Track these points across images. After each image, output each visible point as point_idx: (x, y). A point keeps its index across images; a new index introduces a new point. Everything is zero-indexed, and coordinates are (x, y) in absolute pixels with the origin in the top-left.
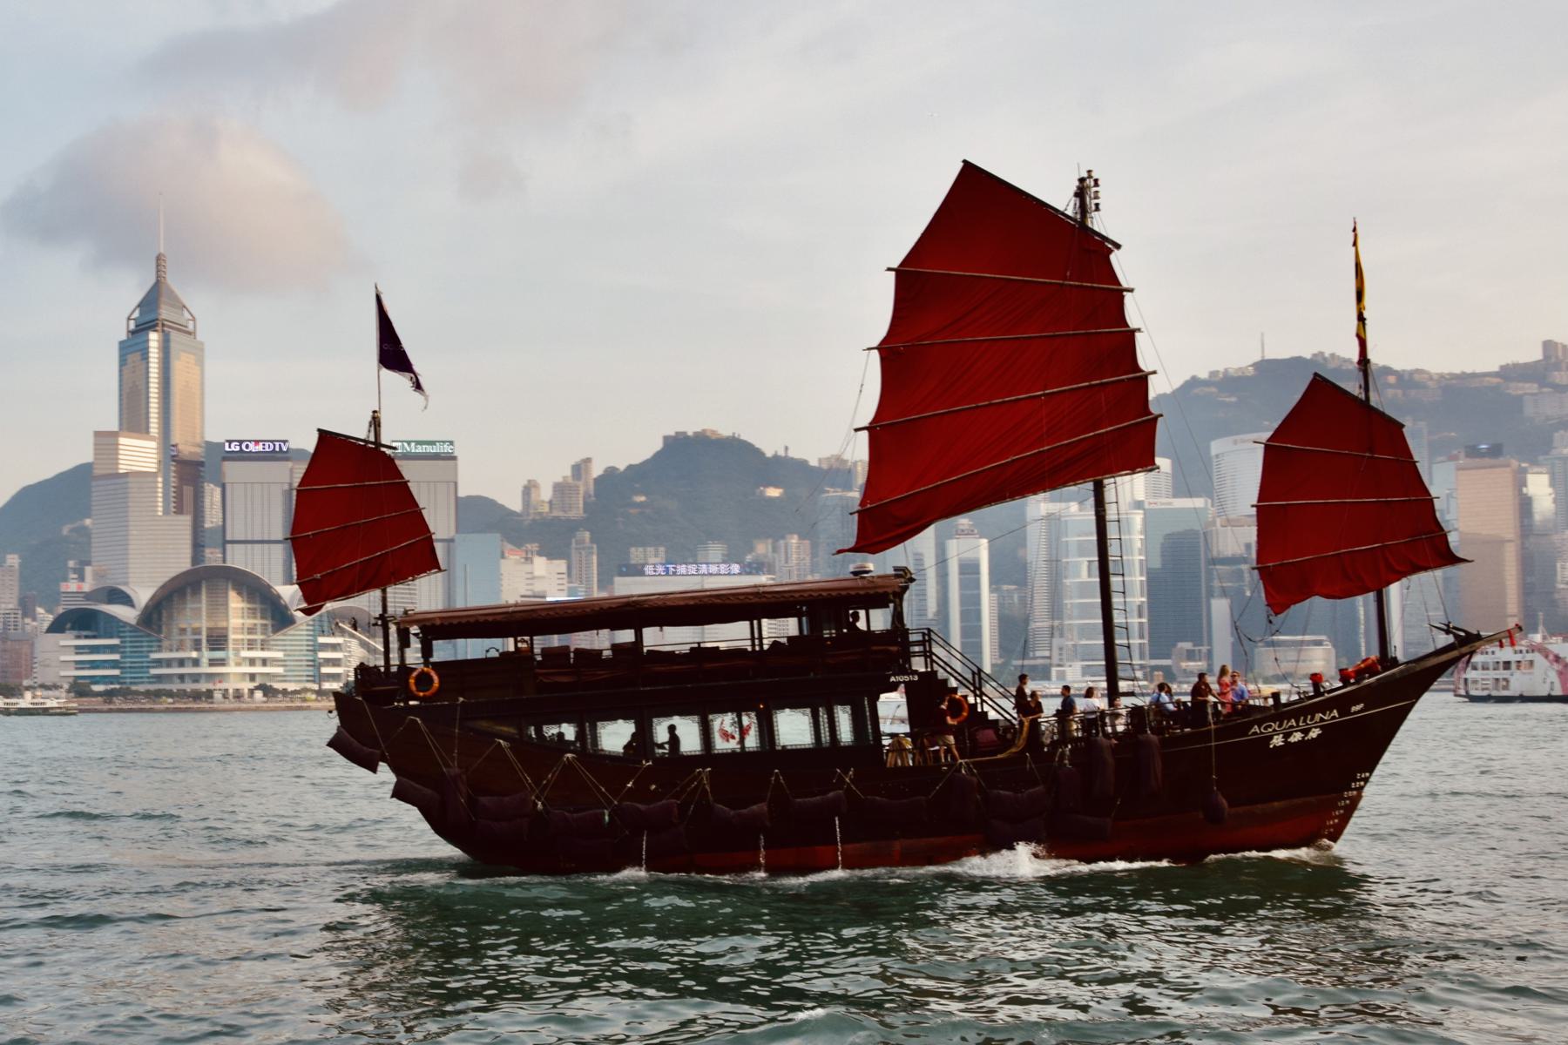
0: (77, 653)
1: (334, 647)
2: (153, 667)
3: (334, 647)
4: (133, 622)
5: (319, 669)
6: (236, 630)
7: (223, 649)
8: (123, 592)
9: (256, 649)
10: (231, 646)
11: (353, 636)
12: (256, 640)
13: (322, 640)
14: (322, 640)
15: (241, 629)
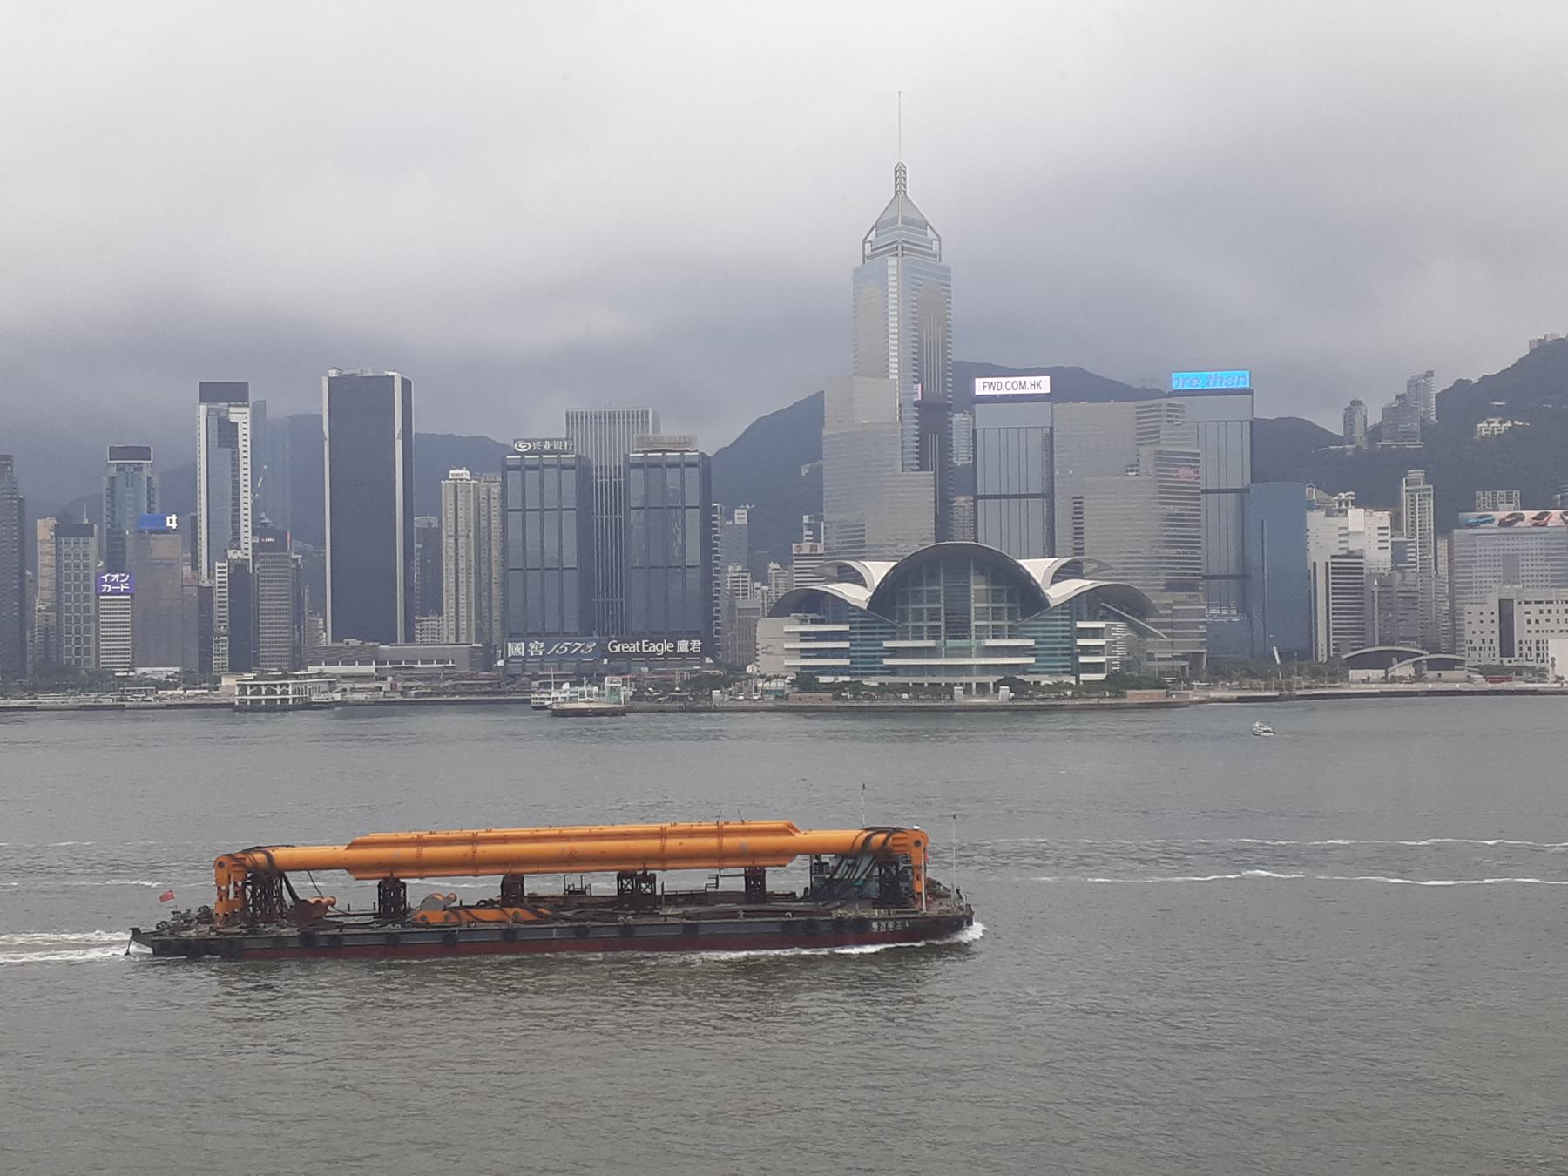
0: (802, 640)
1: (1096, 633)
2: (888, 657)
3: (1096, 633)
4: (864, 606)
5: (1077, 659)
6: (981, 614)
7: (963, 638)
8: (857, 571)
9: (1004, 638)
10: (973, 632)
11: (1120, 618)
12: (1003, 626)
13: (1080, 625)
14: (1080, 625)
15: (981, 614)
